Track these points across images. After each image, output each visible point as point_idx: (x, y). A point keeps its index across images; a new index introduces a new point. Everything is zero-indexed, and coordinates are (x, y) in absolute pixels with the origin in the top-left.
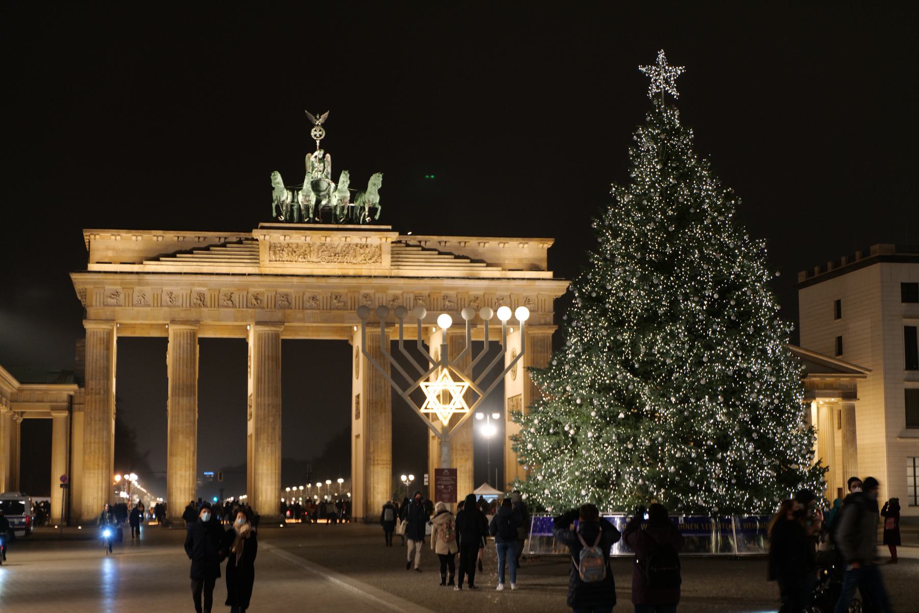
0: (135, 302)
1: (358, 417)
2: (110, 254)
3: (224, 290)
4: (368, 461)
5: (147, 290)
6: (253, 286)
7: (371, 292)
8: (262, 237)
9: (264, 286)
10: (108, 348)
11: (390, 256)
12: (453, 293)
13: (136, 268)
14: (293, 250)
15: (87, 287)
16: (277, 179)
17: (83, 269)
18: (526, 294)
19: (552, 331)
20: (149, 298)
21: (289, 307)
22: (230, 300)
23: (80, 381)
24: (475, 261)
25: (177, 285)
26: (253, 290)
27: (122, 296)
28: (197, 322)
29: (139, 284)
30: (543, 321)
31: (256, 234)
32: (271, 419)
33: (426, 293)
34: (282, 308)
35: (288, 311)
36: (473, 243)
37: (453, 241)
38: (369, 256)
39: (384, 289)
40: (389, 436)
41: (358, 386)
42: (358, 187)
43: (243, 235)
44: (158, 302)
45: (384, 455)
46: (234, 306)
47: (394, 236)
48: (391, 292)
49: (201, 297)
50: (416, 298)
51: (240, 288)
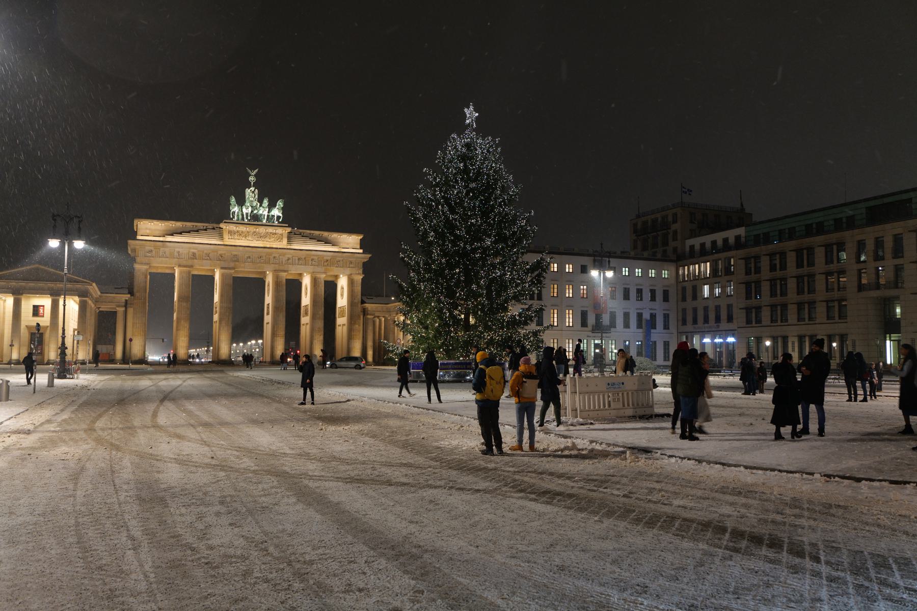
1: (268, 314)
2: (148, 231)
4: (274, 335)
5: (167, 250)
7: (277, 255)
10: (146, 277)
13: (161, 239)
14: (240, 234)
16: (233, 200)
17: (135, 239)
20: (168, 253)
23: (131, 293)
24: (327, 242)
26: (220, 252)
28: (192, 266)
29: (163, 247)
31: (222, 225)
36: (326, 234)
37: (317, 233)
38: (277, 239)
39: (284, 255)
40: (284, 323)
41: (269, 299)
42: (272, 206)
43: (215, 225)
44: (172, 256)
45: (282, 332)
47: (289, 230)
49: (194, 254)
51: (213, 251)
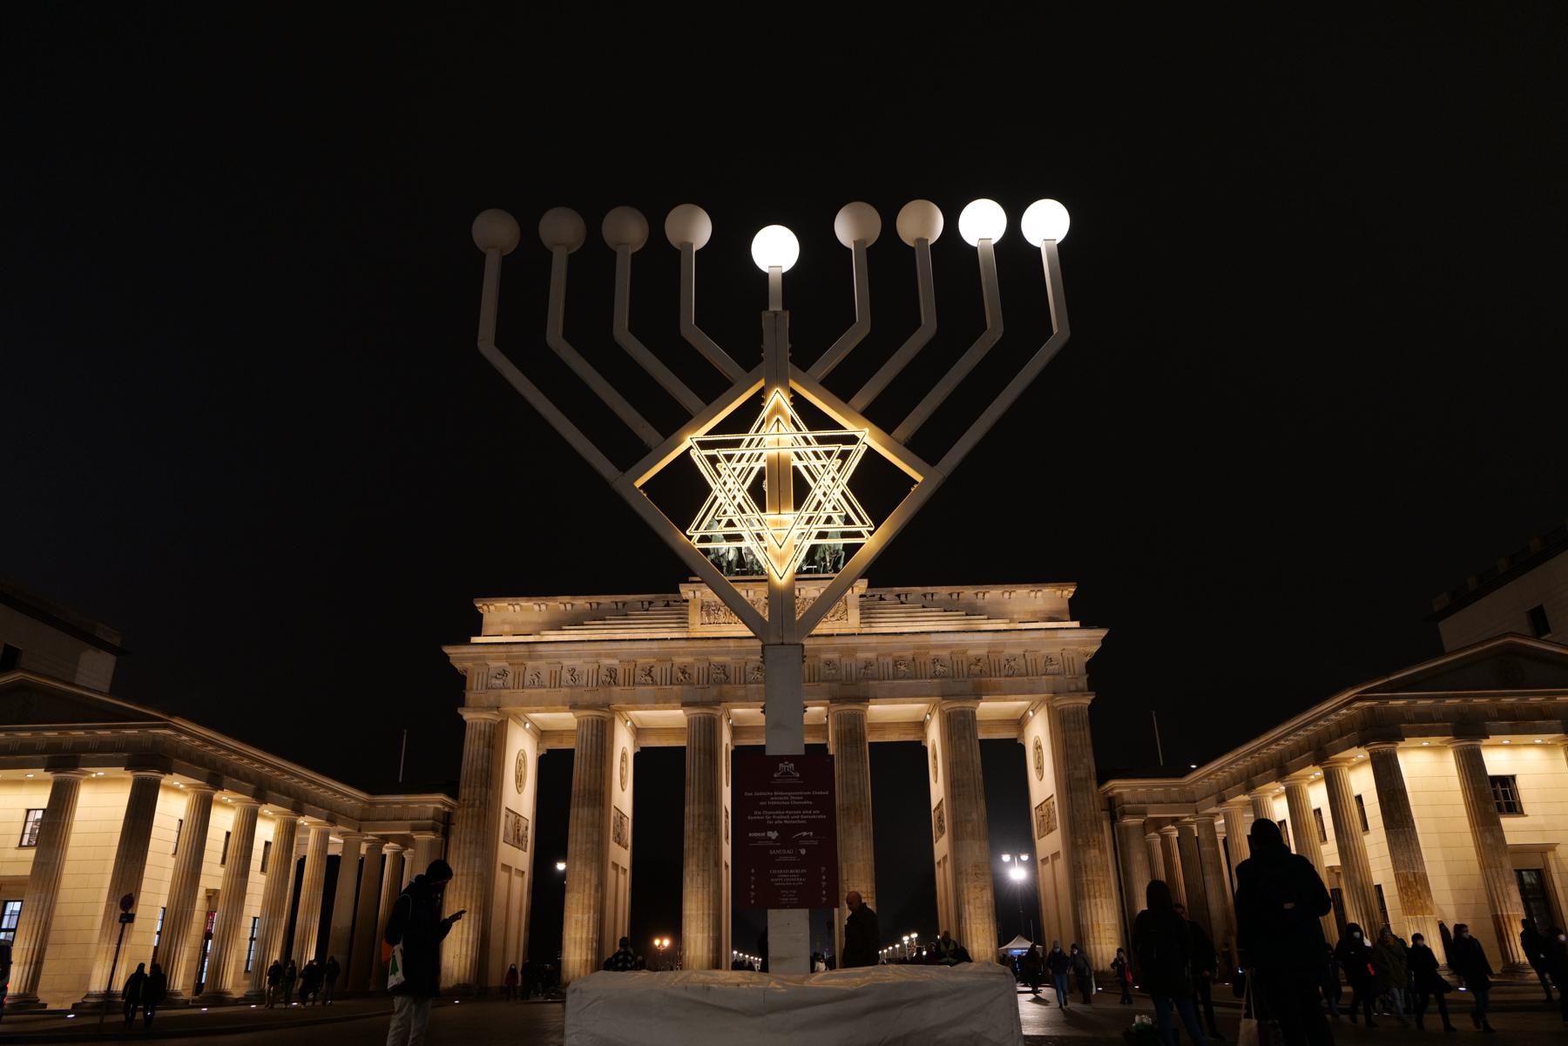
0: (527, 683)
2: (507, 628)
3: (641, 661)
5: (541, 664)
6: (678, 655)
7: (834, 656)
8: (691, 594)
9: (691, 654)
11: (857, 612)
12: (945, 653)
15: (469, 664)
18: (1045, 651)
19: (1086, 701)
20: (545, 676)
21: (727, 680)
22: (649, 674)
23: (454, 793)
24: (972, 611)
25: (579, 656)
26: (678, 660)
27: (510, 676)
29: (531, 657)
30: (1073, 687)
32: (702, 836)
33: (909, 654)
34: (718, 682)
35: (726, 687)
36: (968, 592)
37: (942, 592)
39: (851, 651)
43: (670, 596)
44: (556, 681)
46: (654, 682)
48: (861, 655)
49: (612, 672)
50: (896, 663)
